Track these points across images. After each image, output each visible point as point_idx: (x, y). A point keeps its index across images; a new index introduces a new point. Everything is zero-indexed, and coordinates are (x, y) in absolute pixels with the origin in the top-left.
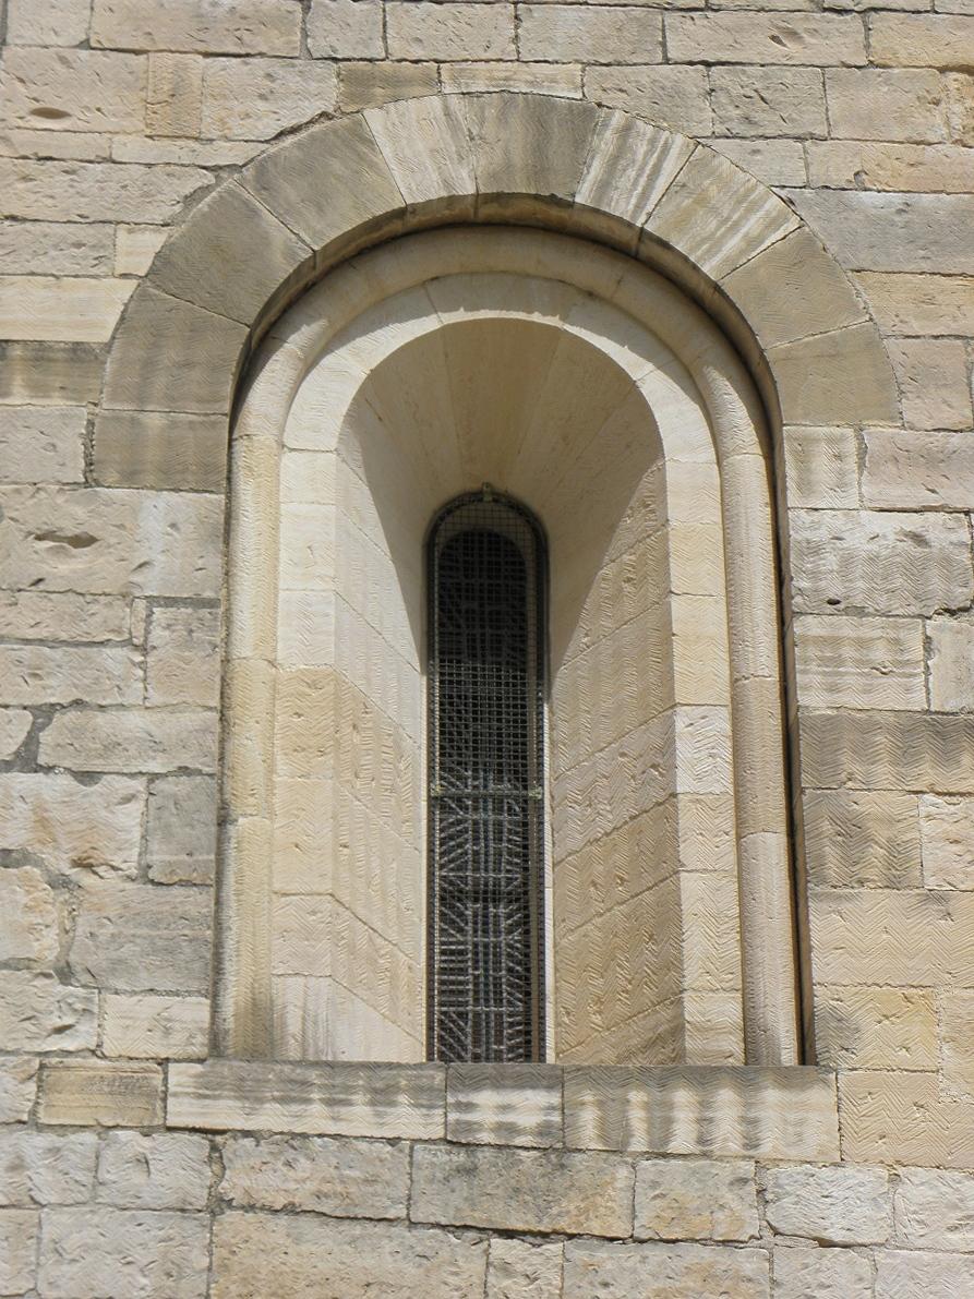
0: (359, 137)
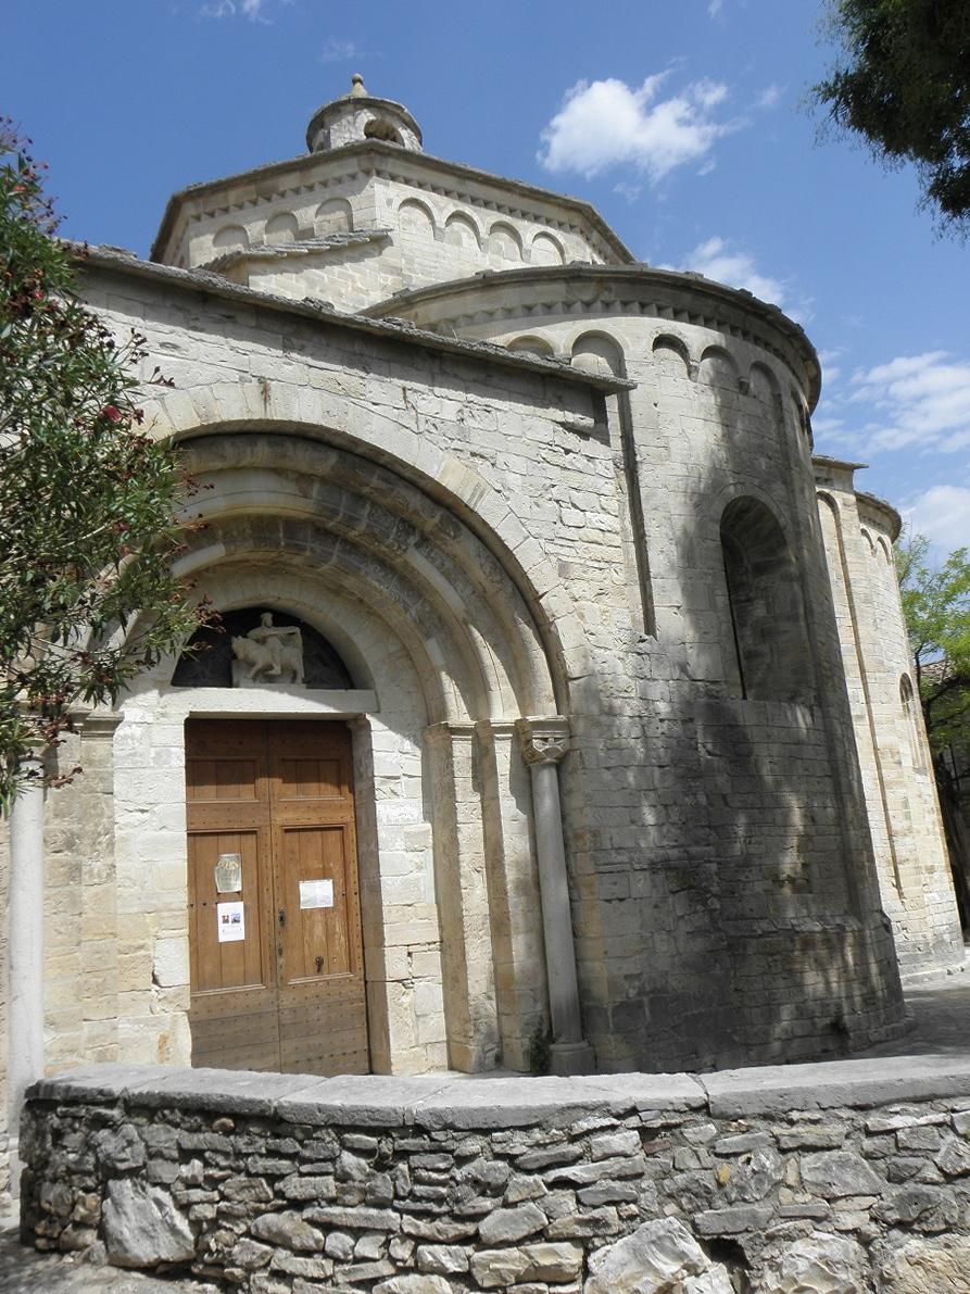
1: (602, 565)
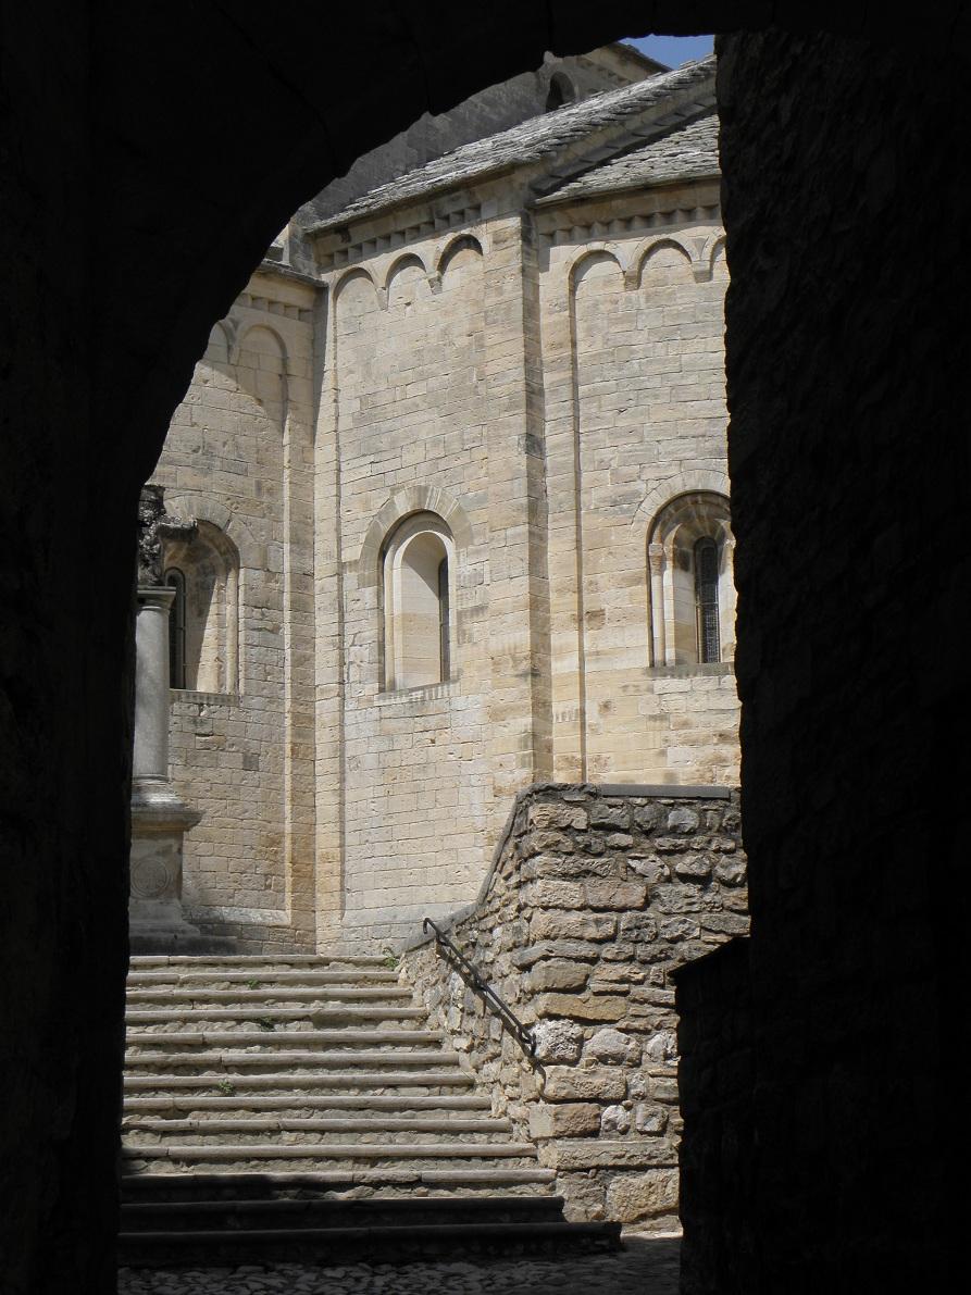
0: (393, 503)
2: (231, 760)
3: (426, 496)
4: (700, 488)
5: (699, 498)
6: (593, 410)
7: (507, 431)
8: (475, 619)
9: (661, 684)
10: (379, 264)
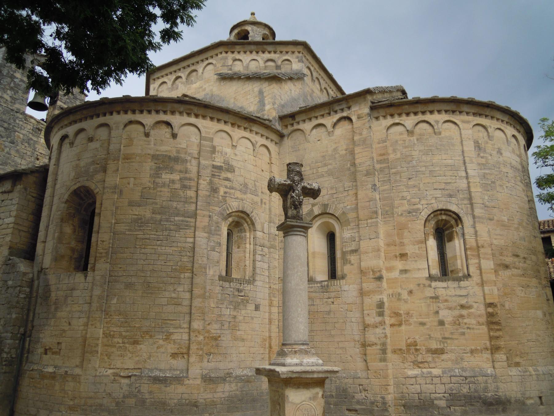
1: (4, 236)
2: (251, 307)
3: (327, 207)
4: (444, 208)
5: (443, 212)
6: (398, 178)
7: (366, 183)
8: (352, 255)
9: (434, 284)
10: (307, 126)
